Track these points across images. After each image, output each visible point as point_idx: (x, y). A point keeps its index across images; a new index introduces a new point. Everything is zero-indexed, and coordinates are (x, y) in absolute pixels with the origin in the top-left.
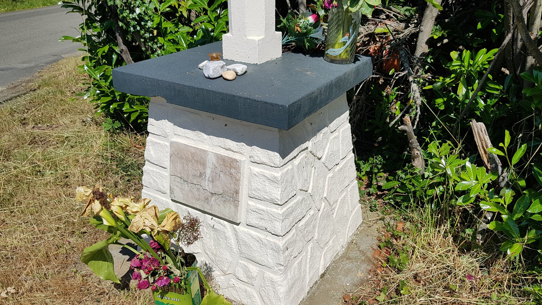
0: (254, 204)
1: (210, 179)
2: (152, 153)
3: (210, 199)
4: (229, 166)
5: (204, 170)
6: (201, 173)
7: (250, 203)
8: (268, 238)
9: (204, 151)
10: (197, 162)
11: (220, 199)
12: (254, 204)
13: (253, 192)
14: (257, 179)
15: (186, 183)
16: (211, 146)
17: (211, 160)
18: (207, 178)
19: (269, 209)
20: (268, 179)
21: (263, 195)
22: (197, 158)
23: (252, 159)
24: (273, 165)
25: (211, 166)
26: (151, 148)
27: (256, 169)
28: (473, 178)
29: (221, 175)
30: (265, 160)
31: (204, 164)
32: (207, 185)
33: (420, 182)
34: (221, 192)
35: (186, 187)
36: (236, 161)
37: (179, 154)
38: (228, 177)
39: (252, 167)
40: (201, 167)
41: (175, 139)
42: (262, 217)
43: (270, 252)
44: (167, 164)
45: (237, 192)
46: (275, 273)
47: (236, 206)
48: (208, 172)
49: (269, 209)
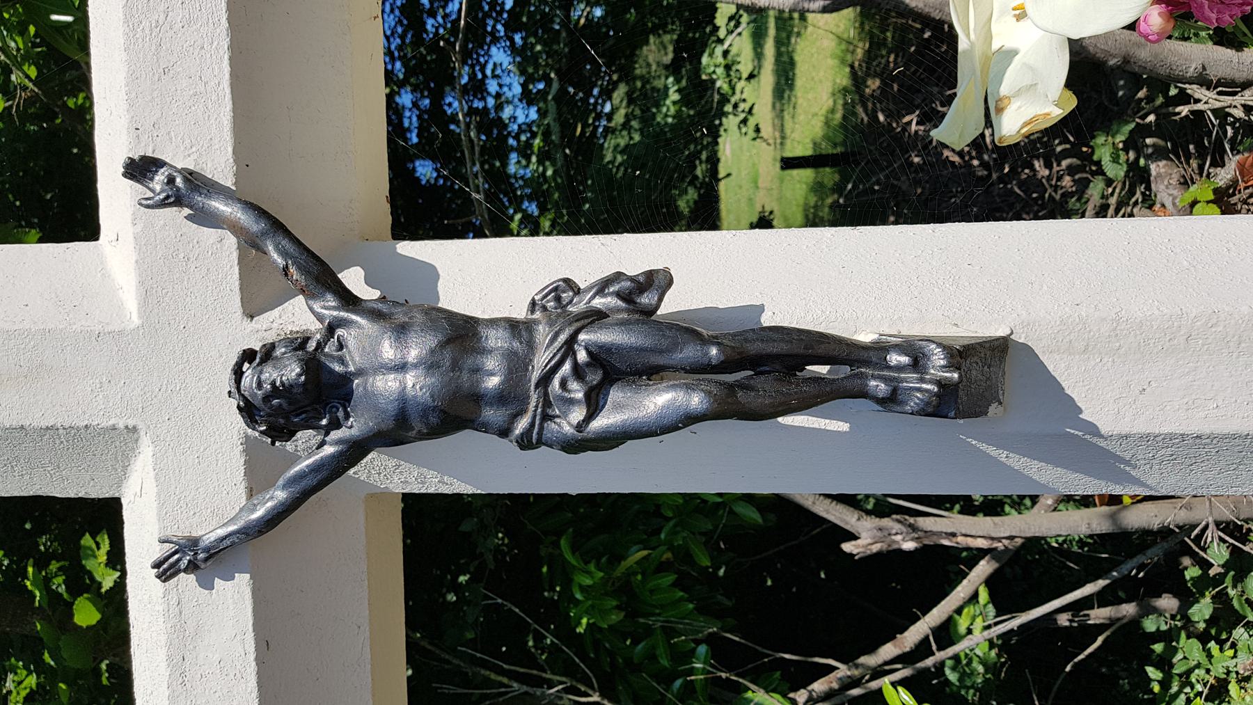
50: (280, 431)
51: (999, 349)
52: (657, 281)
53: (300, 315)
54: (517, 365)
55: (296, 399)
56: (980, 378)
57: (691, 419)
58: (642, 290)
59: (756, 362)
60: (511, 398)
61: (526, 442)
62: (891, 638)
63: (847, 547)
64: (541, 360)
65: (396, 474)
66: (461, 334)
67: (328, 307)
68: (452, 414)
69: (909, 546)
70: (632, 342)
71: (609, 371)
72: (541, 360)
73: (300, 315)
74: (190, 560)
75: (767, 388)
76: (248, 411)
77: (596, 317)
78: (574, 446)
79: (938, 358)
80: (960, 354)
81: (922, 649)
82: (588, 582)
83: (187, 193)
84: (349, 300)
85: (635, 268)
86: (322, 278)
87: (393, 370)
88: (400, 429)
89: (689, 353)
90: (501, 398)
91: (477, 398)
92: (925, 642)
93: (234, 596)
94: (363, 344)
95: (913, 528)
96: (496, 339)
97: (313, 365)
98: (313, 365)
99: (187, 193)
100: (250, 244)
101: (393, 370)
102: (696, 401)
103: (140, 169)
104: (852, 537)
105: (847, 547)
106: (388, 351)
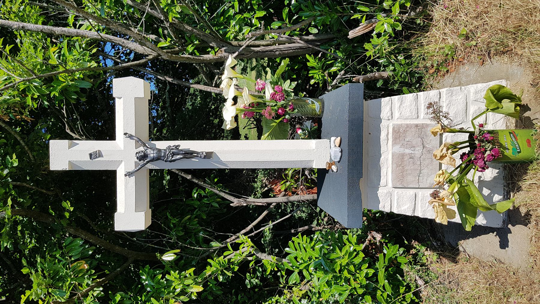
1: (412, 149)
2: (406, 207)
4: (399, 133)
6: (410, 158)
7: (422, 117)
8: (444, 101)
9: (393, 156)
11: (426, 140)
13: (413, 114)
14: (403, 112)
15: (422, 171)
16: (388, 152)
17: (398, 149)
18: (413, 152)
19: (422, 102)
21: (413, 106)
22: (400, 161)
23: (390, 118)
24: (390, 102)
25: (402, 149)
26: (402, 209)
27: (396, 114)
28: (382, 27)
29: (407, 140)
30: (388, 108)
31: (403, 155)
32: (418, 152)
33: (399, 71)
34: (420, 139)
35: (425, 171)
36: (393, 129)
37: (401, 184)
38: (407, 135)
39: (396, 118)
40: (406, 158)
41: (390, 185)
43: (454, 98)
45: (417, 126)
46: (469, 92)
48: (407, 151)
49: (422, 102)
50: (140, 160)
51: (212, 152)
52: (179, 146)
53: (142, 149)
54: (165, 153)
55: (143, 157)
56: (209, 155)
57: (181, 158)
58: (177, 147)
59: (188, 153)
60: (164, 156)
61: (166, 161)
62: (244, 228)
63: (231, 205)
64: (167, 153)
65: (150, 166)
66: (159, 150)
67: (146, 148)
68: (158, 159)
69: (245, 204)
70: (176, 151)
71: (174, 154)
72: (167, 153)
73: (142, 149)
74: (129, 174)
75: (189, 156)
76: (137, 158)
77: (173, 149)
78: (171, 161)
79: (204, 153)
80: (206, 153)
81: (251, 231)
82: (175, 222)
83: (131, 137)
84: (148, 147)
85: (177, 145)
86: (145, 145)
87: (152, 154)
88: (153, 160)
89: (181, 152)
90: (163, 156)
91: (161, 156)
92: (252, 229)
93: (133, 178)
94: (149, 151)
95: (246, 201)
96: (163, 151)
97: (144, 154)
98: (144, 154)
99: (131, 137)
100: (137, 142)
101: (152, 154)
102: (182, 156)
103: (125, 134)
104: (232, 203)
105: (231, 205)
106: (152, 152)
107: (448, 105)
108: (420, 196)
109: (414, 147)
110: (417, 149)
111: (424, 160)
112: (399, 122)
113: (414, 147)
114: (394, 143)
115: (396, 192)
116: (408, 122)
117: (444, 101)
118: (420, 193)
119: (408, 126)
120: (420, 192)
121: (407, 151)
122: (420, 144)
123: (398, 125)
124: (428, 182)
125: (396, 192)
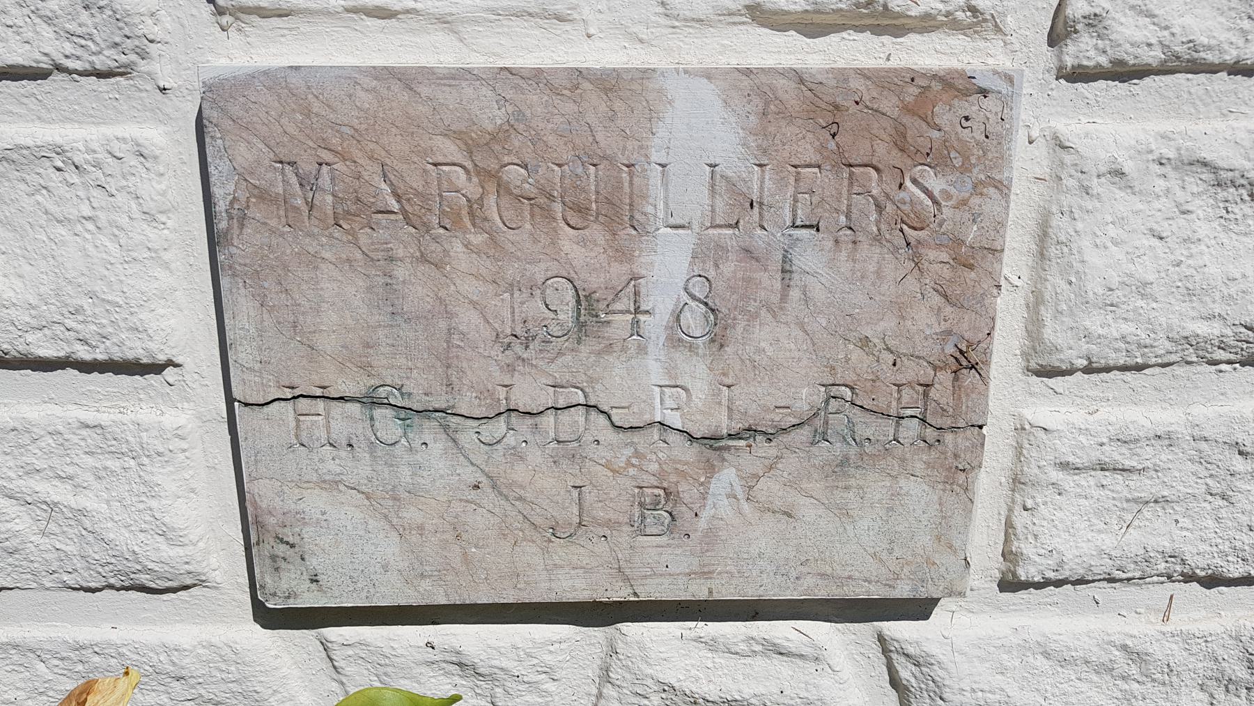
0: (1078, 417)
1: (694, 319)
3: (687, 491)
5: (623, 254)
6: (585, 302)
9: (609, 83)
10: (538, 204)
11: (791, 463)
12: (1078, 417)
13: (1094, 322)
14: (1123, 202)
15: (429, 431)
18: (655, 326)
20: (1219, 178)
23: (1083, 50)
27: (1111, 126)
31: (614, 210)
32: (658, 381)
34: (806, 398)
35: (433, 461)
36: (959, 86)
38: (871, 255)
39: (1068, 127)
40: (582, 252)
42: (1145, 486)
44: (175, 317)
45: (968, 361)
47: (957, 475)
48: (667, 266)
107: (1137, 656)
108: (145, 414)
109: (718, 341)
110: (697, 374)
111: (568, 451)
112: (1026, 163)
113: (718, 341)
114: (760, 95)
115: (152, 135)
116: (1015, 264)
117: (1178, 621)
118: (174, 418)
119: (973, 258)
120: (184, 414)
121: (667, 266)
122: (756, 399)
123: (995, 139)
124: (315, 502)
125: (152, 135)
